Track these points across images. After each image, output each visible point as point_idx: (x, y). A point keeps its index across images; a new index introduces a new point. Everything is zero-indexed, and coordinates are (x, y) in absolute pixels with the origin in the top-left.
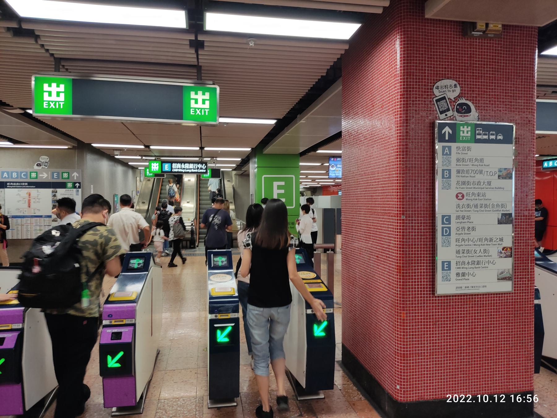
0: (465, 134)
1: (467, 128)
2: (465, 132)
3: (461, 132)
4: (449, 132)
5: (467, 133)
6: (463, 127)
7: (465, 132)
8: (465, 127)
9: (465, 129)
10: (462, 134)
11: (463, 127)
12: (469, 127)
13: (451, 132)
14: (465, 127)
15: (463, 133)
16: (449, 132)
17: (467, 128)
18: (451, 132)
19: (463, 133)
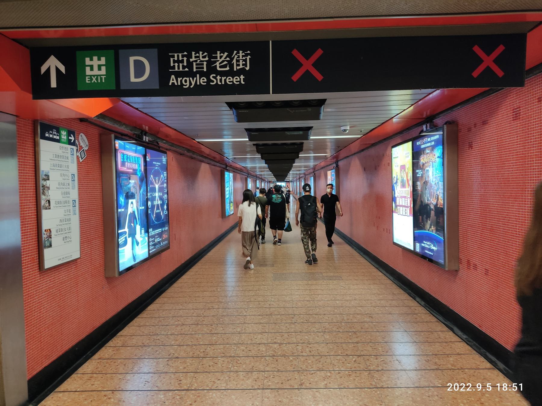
0: (96, 72)
1: (99, 59)
2: (96, 68)
3: (88, 69)
4: (57, 70)
5: (100, 69)
6: (91, 60)
7: (96, 68)
8: (95, 58)
9: (95, 62)
10: (88, 72)
11: (91, 60)
12: (103, 59)
13: (62, 69)
14: (95, 58)
15: (92, 69)
16: (57, 70)
17: (99, 59)
18: (62, 69)
19: (92, 69)
